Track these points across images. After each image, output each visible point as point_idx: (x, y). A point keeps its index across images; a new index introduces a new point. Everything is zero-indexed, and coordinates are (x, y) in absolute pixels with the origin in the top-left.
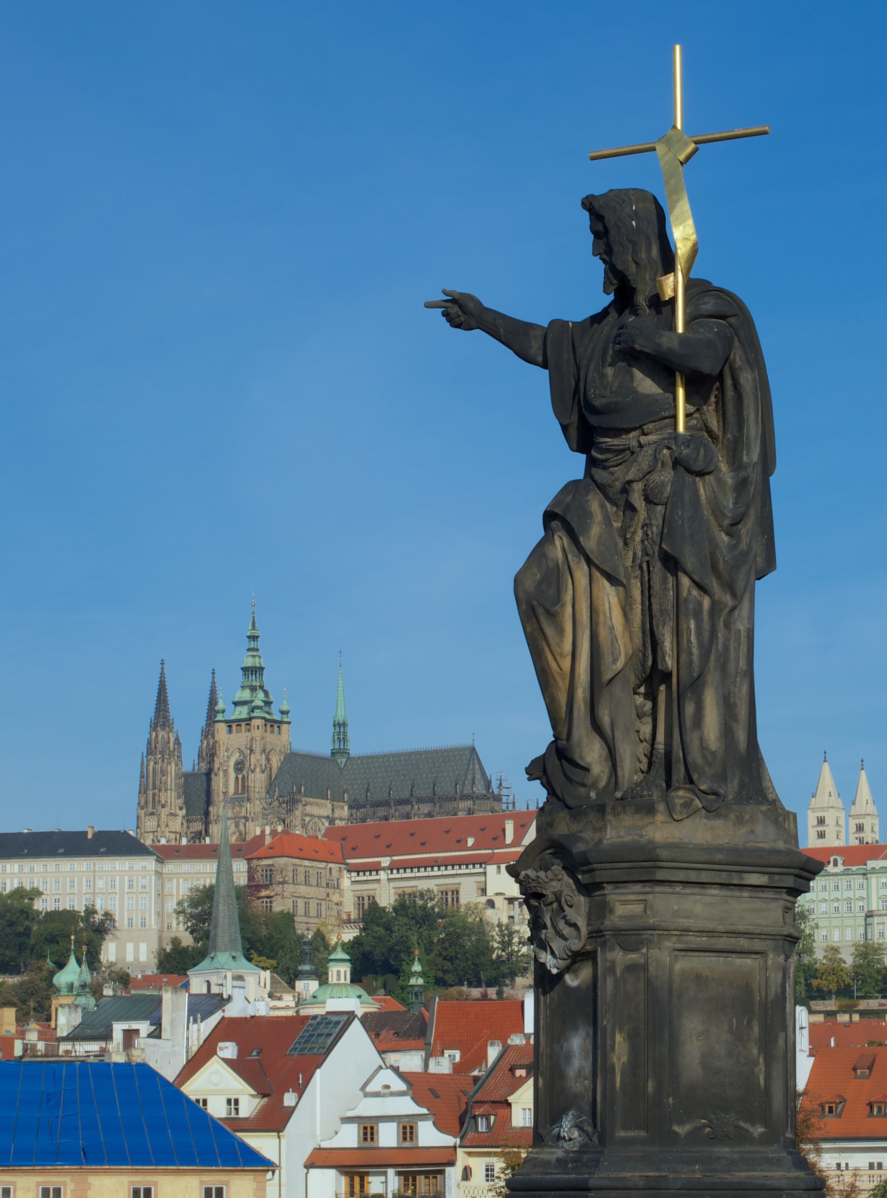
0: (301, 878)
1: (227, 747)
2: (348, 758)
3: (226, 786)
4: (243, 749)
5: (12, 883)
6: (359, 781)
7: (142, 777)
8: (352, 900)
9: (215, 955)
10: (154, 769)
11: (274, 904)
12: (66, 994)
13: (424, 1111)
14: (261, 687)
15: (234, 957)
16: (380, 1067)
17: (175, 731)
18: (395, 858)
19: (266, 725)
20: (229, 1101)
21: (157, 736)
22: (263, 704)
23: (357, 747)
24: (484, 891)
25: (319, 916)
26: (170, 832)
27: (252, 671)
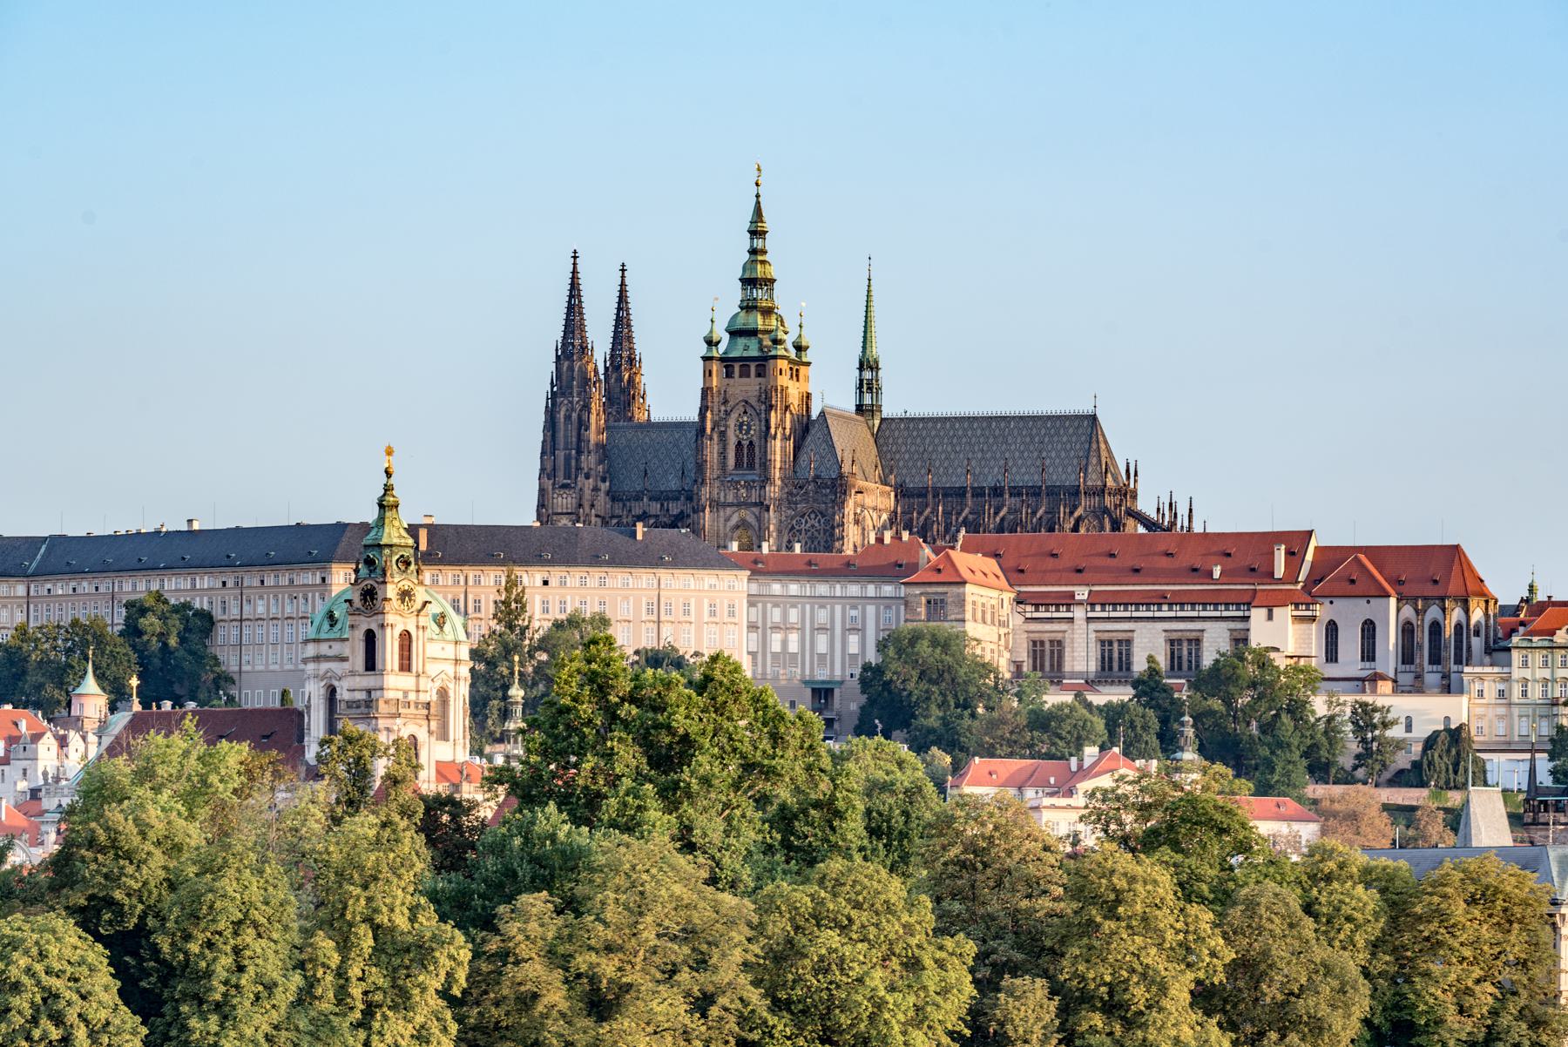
0: (979, 615)
2: (883, 420)
4: (753, 401)
6: (907, 456)
8: (1025, 645)
10: (568, 418)
21: (571, 369)
23: (893, 404)
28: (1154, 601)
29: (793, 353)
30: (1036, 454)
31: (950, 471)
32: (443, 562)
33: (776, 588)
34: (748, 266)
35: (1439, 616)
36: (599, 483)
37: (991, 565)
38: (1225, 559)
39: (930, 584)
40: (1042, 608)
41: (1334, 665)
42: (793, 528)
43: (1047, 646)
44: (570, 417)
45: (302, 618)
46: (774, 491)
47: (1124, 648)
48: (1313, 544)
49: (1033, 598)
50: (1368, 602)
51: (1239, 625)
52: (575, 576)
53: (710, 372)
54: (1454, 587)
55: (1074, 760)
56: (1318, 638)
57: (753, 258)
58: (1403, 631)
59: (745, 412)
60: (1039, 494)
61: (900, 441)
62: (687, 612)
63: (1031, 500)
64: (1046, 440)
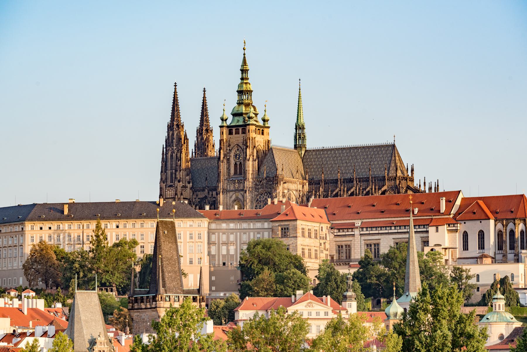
0: (306, 234)
1: (229, 144)
2: (306, 151)
3: (229, 169)
4: (241, 145)
6: (315, 167)
8: (335, 248)
9: (409, 294)
10: (172, 156)
12: (393, 318)
17: (185, 131)
19: (256, 129)
21: (173, 134)
23: (311, 144)
26: (184, 198)
27: (245, 93)
28: (389, 225)
29: (261, 123)
30: (368, 163)
31: (332, 172)
32: (73, 219)
33: (224, 225)
34: (240, 85)
35: (513, 227)
36: (187, 184)
37: (322, 212)
38: (421, 205)
39: (282, 221)
40: (341, 231)
41: (467, 251)
42: (258, 200)
43: (344, 247)
44: (172, 155)
45: (14, 246)
46: (249, 183)
47: (376, 247)
48: (460, 197)
49: (337, 226)
50: (481, 222)
51: (425, 235)
52: (130, 223)
53: (223, 133)
54: (520, 214)
55: (293, 297)
56: (459, 240)
57: (242, 81)
58: (498, 235)
59: (238, 150)
60: (368, 181)
61: (313, 160)
63: (363, 185)
64: (373, 156)
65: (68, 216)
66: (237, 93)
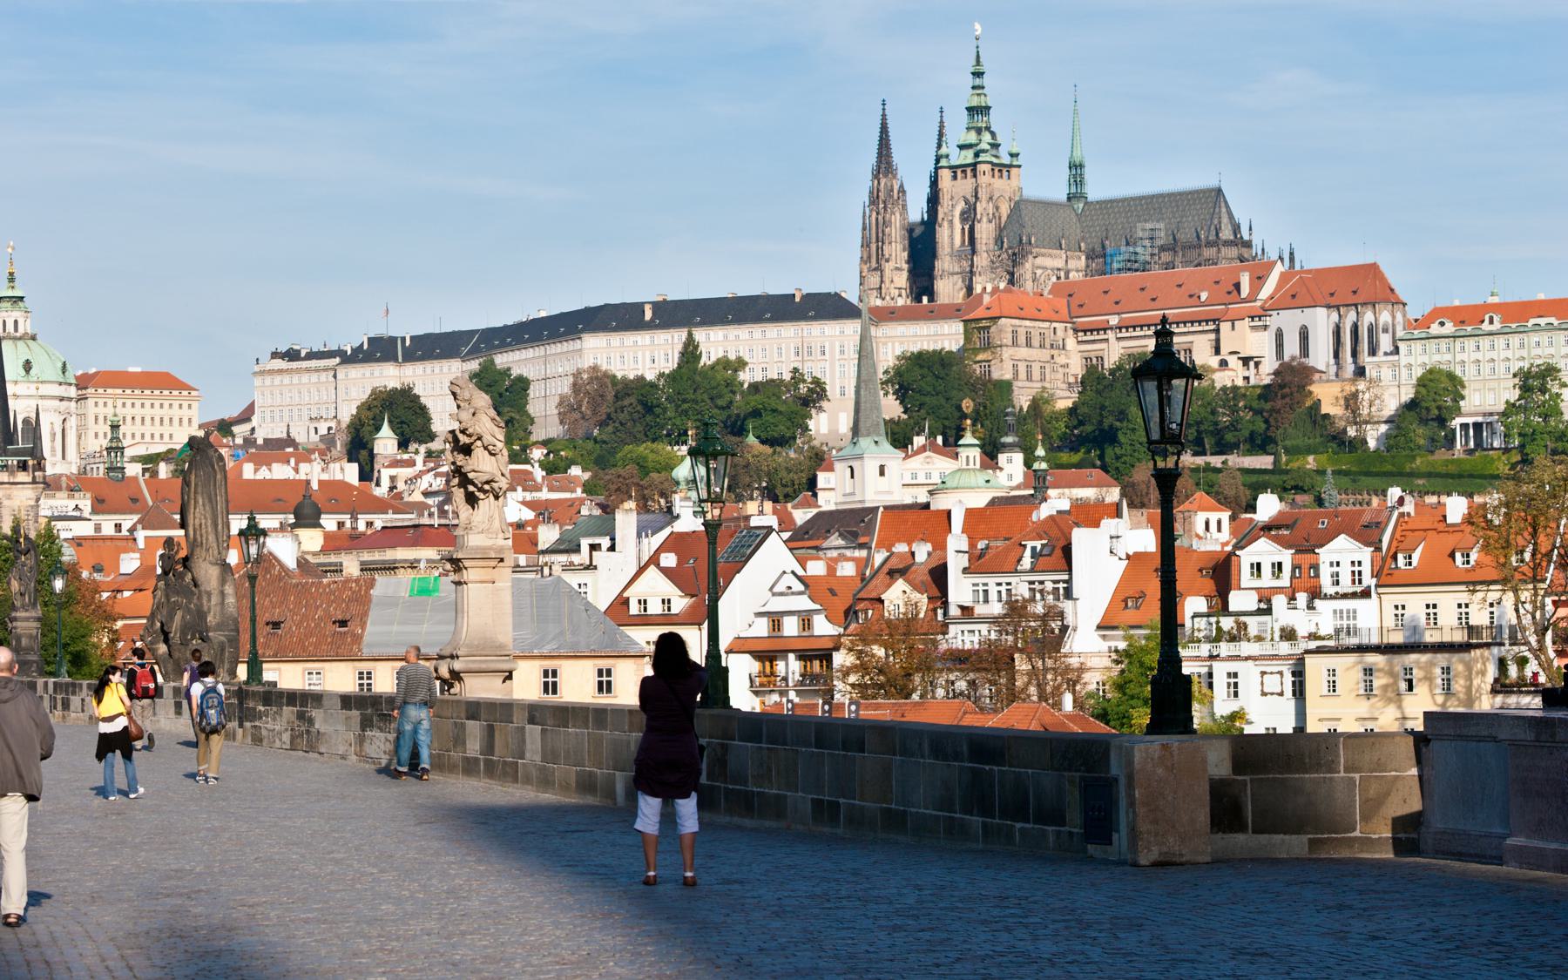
0: (1022, 339)
2: (1086, 203)
3: (952, 237)
5: (717, 352)
7: (864, 229)
10: (877, 219)
11: (992, 369)
13: (818, 607)
14: (988, 129)
15: (876, 442)
16: (784, 572)
18: (1124, 316)
19: (993, 170)
20: (663, 601)
21: (879, 183)
22: (988, 147)
24: (1217, 351)
25: (1043, 379)
40: (1089, 333)
62: (823, 353)
65: (652, 320)
66: (966, 112)
